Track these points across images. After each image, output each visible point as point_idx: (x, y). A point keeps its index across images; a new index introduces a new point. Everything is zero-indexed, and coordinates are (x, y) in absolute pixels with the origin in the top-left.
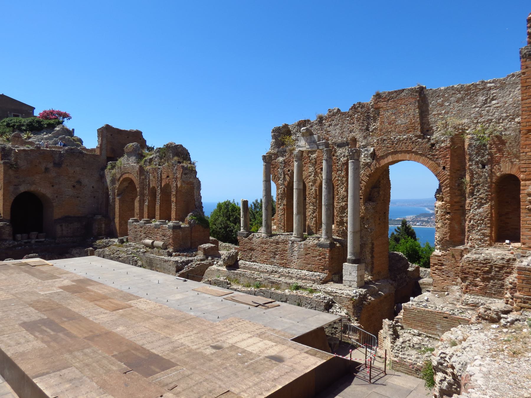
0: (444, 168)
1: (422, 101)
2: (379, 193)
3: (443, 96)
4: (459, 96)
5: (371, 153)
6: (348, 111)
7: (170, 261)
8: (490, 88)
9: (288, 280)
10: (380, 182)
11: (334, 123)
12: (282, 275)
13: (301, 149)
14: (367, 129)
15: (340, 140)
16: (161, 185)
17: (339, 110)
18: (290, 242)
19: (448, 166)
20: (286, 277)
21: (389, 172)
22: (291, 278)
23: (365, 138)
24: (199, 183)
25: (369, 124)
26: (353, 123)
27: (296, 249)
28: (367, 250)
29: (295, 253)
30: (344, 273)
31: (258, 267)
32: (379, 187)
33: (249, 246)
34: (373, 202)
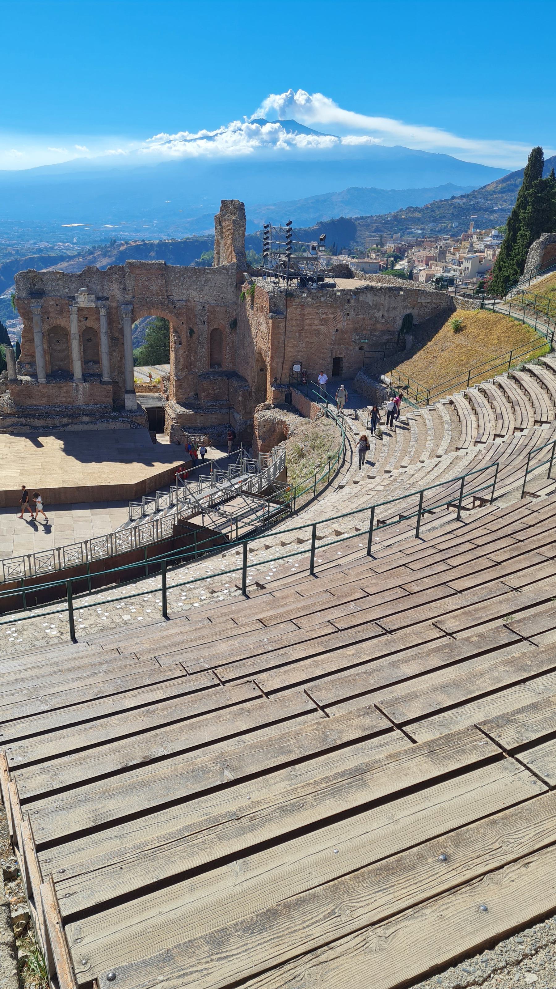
0: (183, 323)
14: (125, 289)
25: (125, 284)
27: (81, 389)
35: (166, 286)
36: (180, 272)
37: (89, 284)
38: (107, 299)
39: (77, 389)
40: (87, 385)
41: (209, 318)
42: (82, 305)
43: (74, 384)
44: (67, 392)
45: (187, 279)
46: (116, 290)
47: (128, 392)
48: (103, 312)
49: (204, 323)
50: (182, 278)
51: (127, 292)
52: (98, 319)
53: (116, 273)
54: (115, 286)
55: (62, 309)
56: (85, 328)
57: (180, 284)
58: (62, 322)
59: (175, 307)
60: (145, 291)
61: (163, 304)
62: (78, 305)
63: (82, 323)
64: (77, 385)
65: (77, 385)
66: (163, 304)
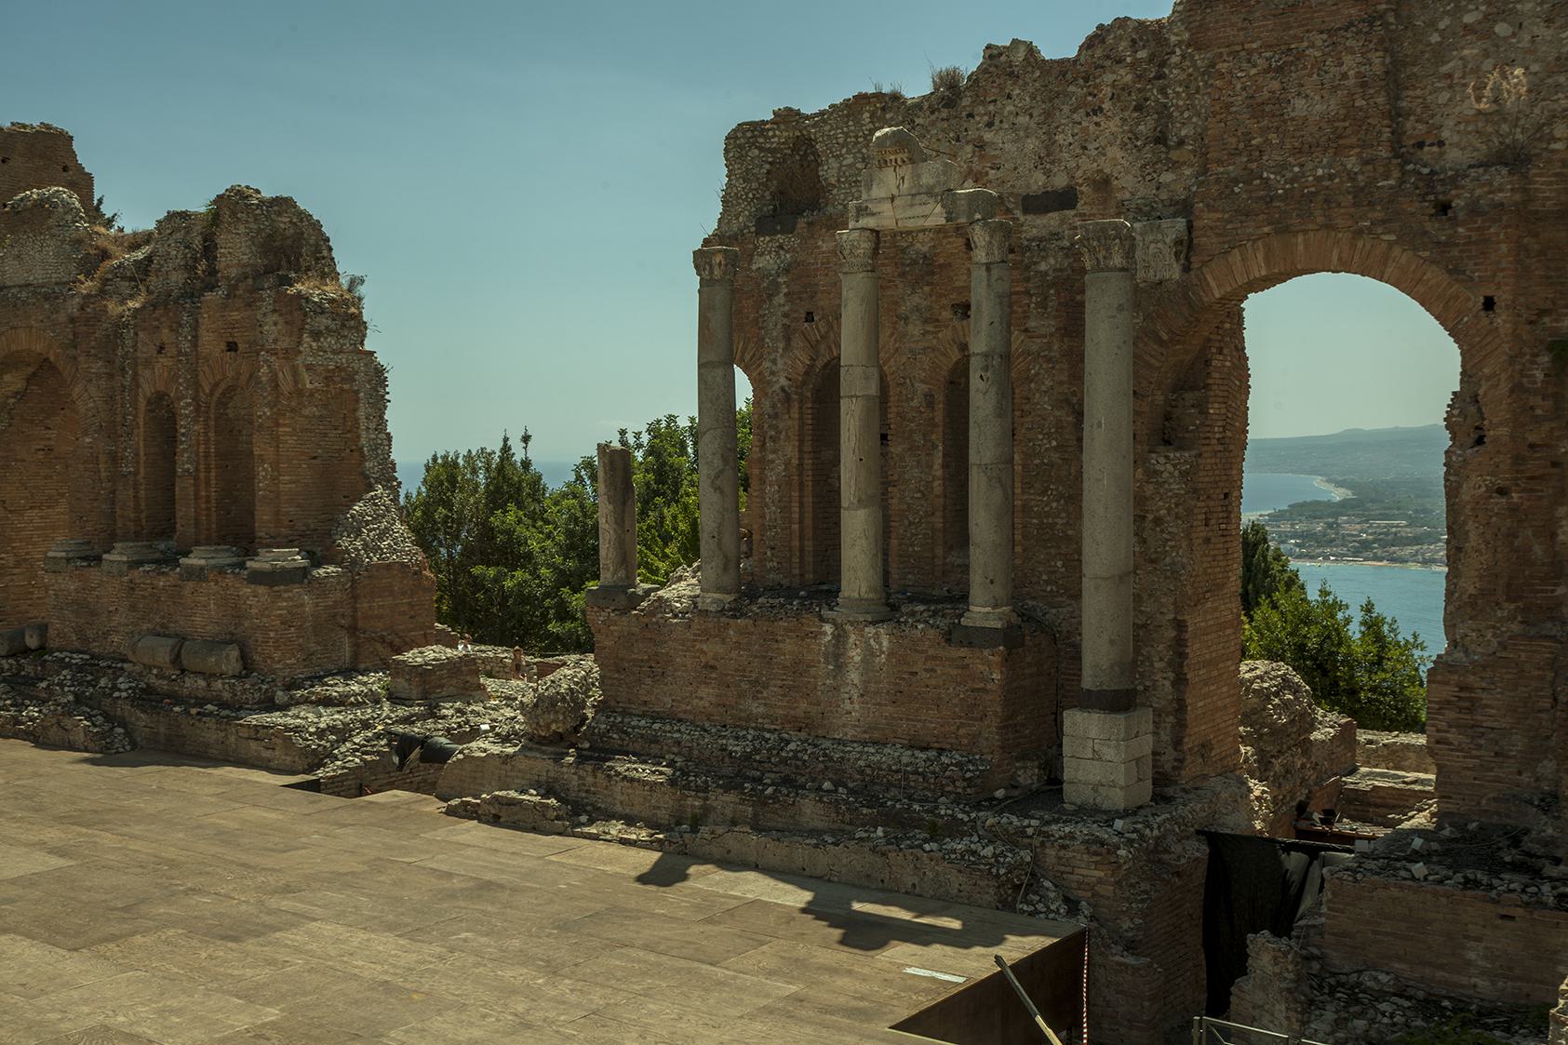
0: (1489, 304)
1: (1397, 16)
2: (1203, 412)
5: (1178, 242)
6: (1072, 54)
10: (1207, 363)
14: (1161, 140)
15: (1037, 182)
17: (1031, 50)
19: (1503, 297)
21: (1241, 320)
24: (378, 376)
25: (1163, 112)
26: (1098, 110)
27: (855, 655)
28: (1160, 652)
29: (854, 676)
30: (1066, 750)
32: (1207, 386)
34: (1181, 448)
37: (988, 136)
38: (1065, 199)
40: (883, 639)
42: (887, 217)
43: (828, 628)
46: (1115, 152)
50: (1502, 29)
51: (1174, 155)
54: (1113, 125)
59: (1444, 208)
60: (1263, 131)
61: (1363, 195)
62: (870, 222)
63: (946, 334)
64: (840, 637)
65: (840, 637)
66: (1363, 195)
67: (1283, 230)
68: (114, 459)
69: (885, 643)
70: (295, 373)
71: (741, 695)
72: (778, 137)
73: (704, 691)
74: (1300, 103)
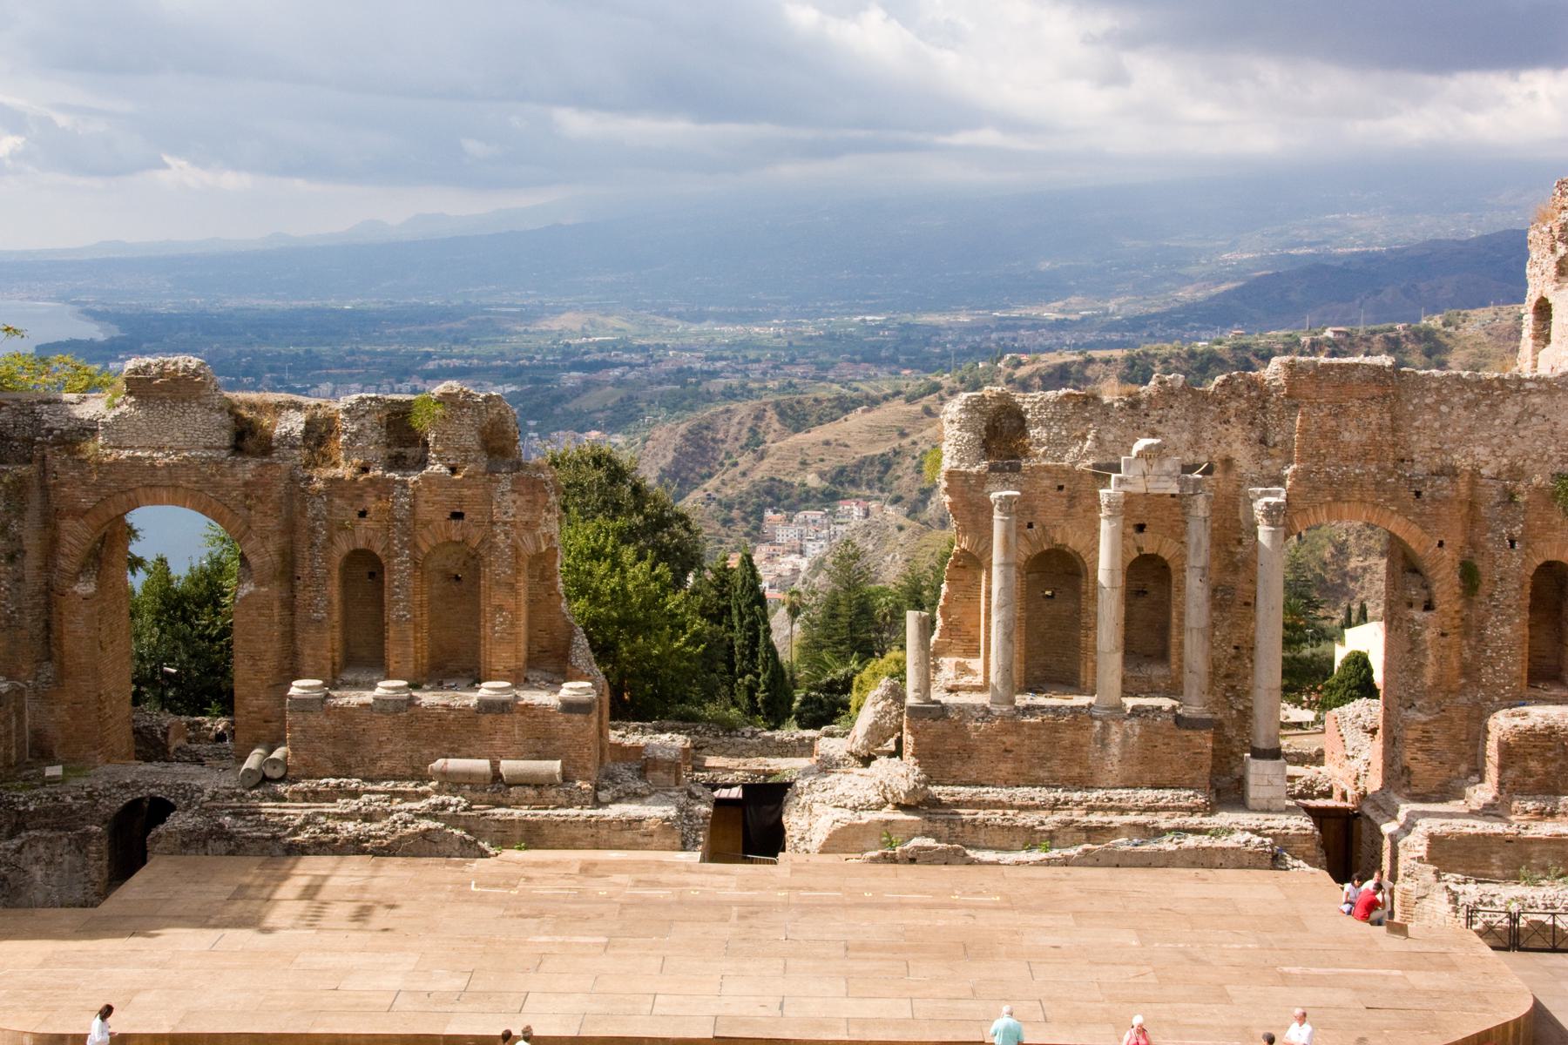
0: (1441, 544)
3: (1438, 390)
4: (1469, 395)
7: (640, 820)
8: (1530, 391)
9: (1117, 820)
11: (1172, 413)
12: (1091, 809)
13: (1129, 488)
14: (1263, 441)
16: (416, 545)
18: (1098, 723)
20: (1104, 809)
22: (1123, 811)
23: (1257, 458)
26: (1227, 422)
27: (1116, 736)
29: (1115, 750)
31: (1005, 799)
33: (953, 744)
35: (1394, 430)
36: (1438, 390)
39: (1103, 742)
41: (1528, 527)
42: (1139, 488)
43: (1098, 723)
44: (1075, 746)
45: (1461, 411)
46: (1237, 445)
47: (1258, 754)
48: (1201, 507)
49: (1512, 546)
50: (1444, 408)
51: (1271, 451)
52: (1178, 531)
53: (1240, 396)
55: (1072, 499)
56: (1136, 554)
57: (1437, 425)
58: (1073, 540)
65: (1106, 728)
67: (1337, 498)
68: (290, 605)
69: (1137, 730)
70: (536, 540)
71: (1032, 767)
72: (995, 404)
73: (1002, 766)
74: (1347, 434)
